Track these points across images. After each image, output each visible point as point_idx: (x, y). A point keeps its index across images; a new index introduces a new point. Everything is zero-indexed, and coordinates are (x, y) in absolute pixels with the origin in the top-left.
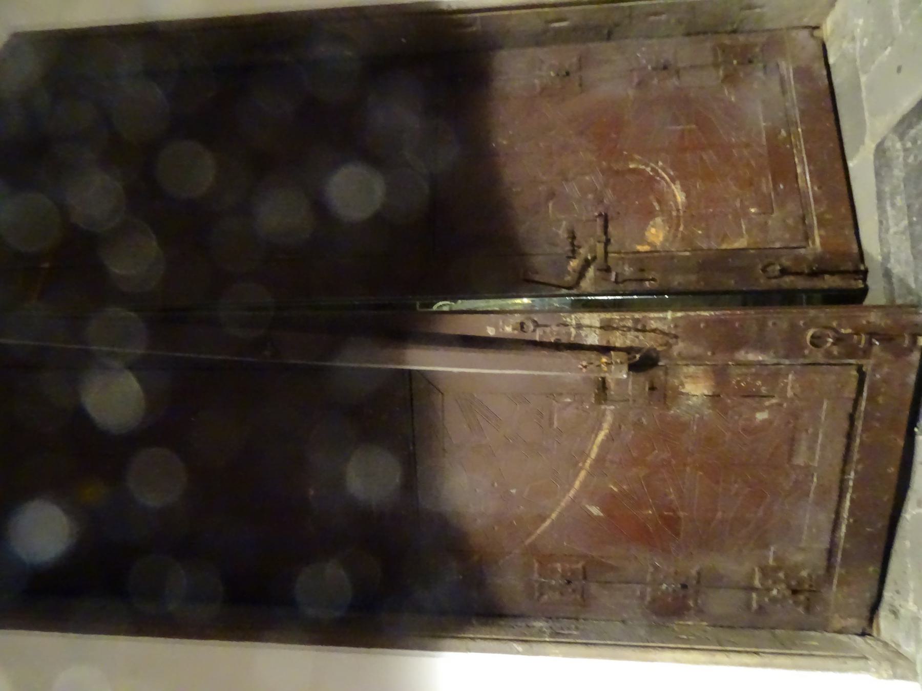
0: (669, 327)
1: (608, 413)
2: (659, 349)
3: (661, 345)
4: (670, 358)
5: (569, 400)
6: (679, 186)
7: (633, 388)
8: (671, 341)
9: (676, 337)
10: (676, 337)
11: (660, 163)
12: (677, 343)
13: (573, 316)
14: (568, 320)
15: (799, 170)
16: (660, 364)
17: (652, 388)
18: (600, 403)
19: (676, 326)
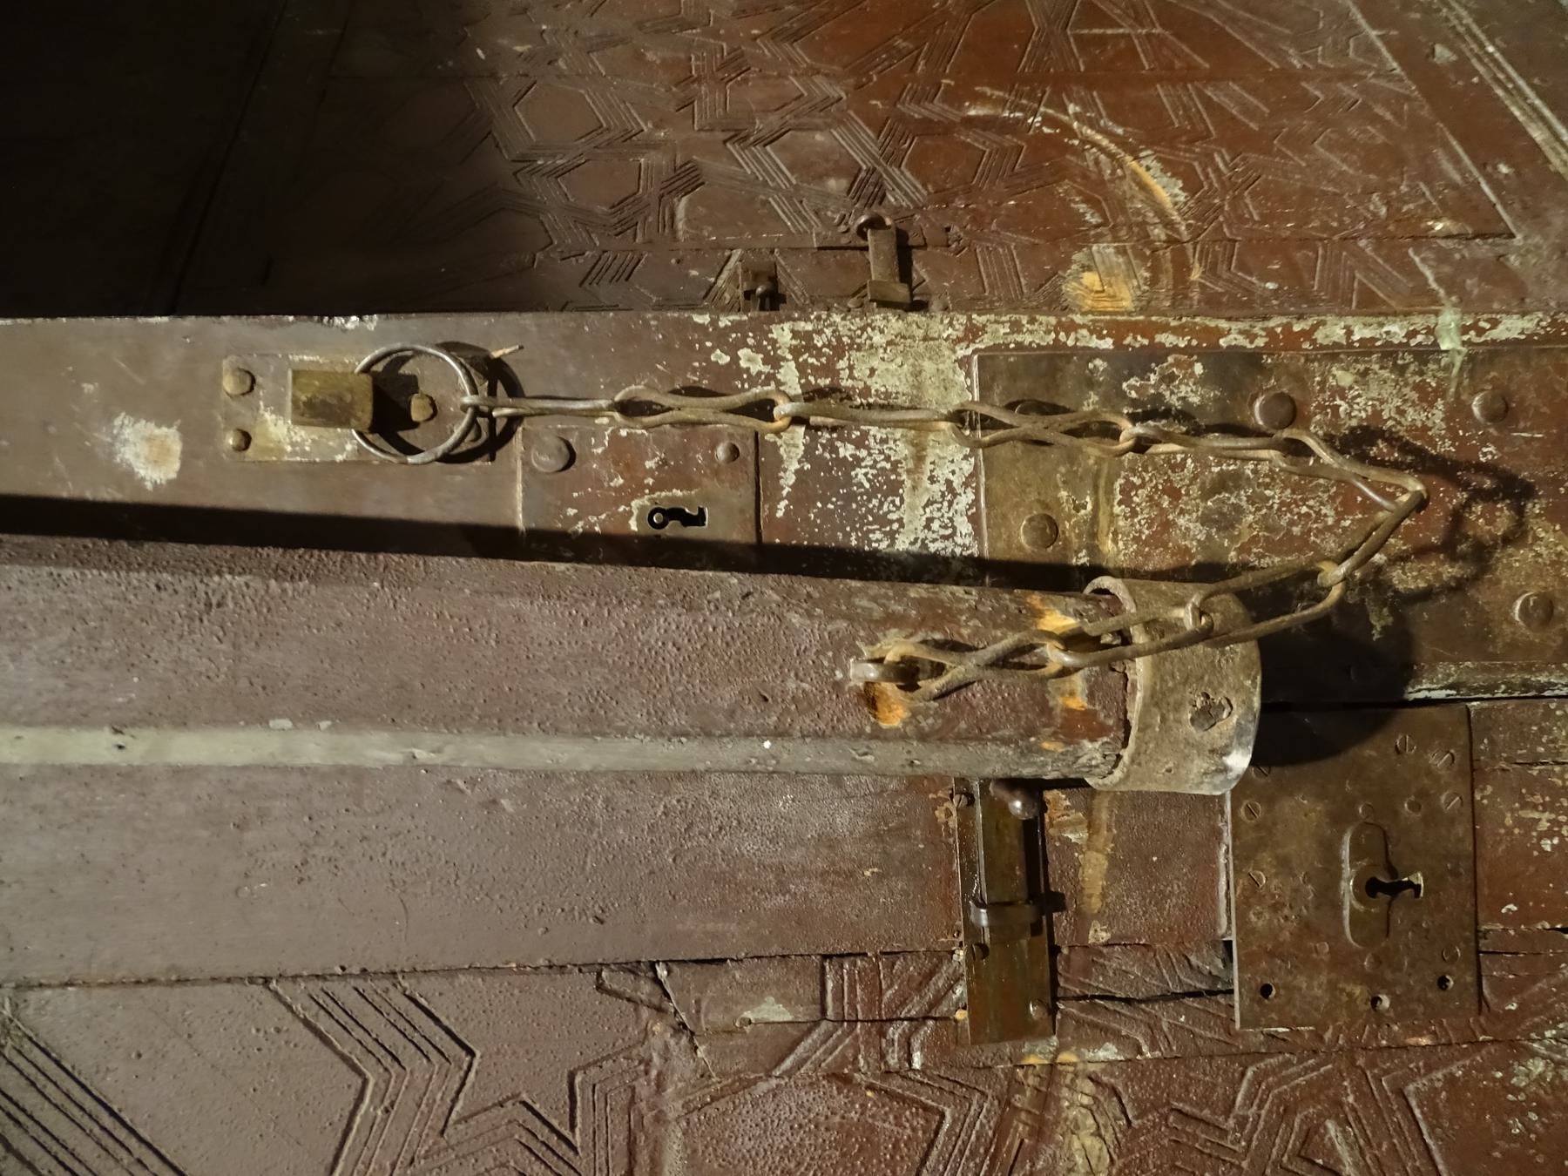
0: (1458, 411)
1: (1076, 1101)
2: (1406, 579)
3: (1423, 552)
4: (1477, 639)
5: (773, 1011)
6: (1154, 164)
7: (1250, 895)
8: (1491, 521)
9: (1514, 490)
10: (1514, 490)
11: (1072, 108)
12: (1517, 536)
13: (783, 334)
14: (751, 361)
15: (1538, 134)
16: (1421, 690)
17: (1382, 886)
18: (1022, 1030)
19: (1503, 413)
